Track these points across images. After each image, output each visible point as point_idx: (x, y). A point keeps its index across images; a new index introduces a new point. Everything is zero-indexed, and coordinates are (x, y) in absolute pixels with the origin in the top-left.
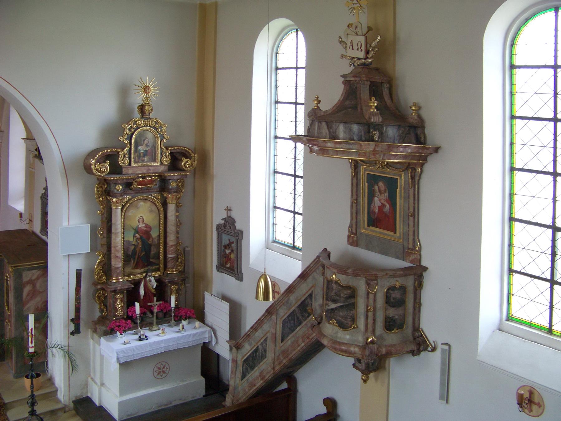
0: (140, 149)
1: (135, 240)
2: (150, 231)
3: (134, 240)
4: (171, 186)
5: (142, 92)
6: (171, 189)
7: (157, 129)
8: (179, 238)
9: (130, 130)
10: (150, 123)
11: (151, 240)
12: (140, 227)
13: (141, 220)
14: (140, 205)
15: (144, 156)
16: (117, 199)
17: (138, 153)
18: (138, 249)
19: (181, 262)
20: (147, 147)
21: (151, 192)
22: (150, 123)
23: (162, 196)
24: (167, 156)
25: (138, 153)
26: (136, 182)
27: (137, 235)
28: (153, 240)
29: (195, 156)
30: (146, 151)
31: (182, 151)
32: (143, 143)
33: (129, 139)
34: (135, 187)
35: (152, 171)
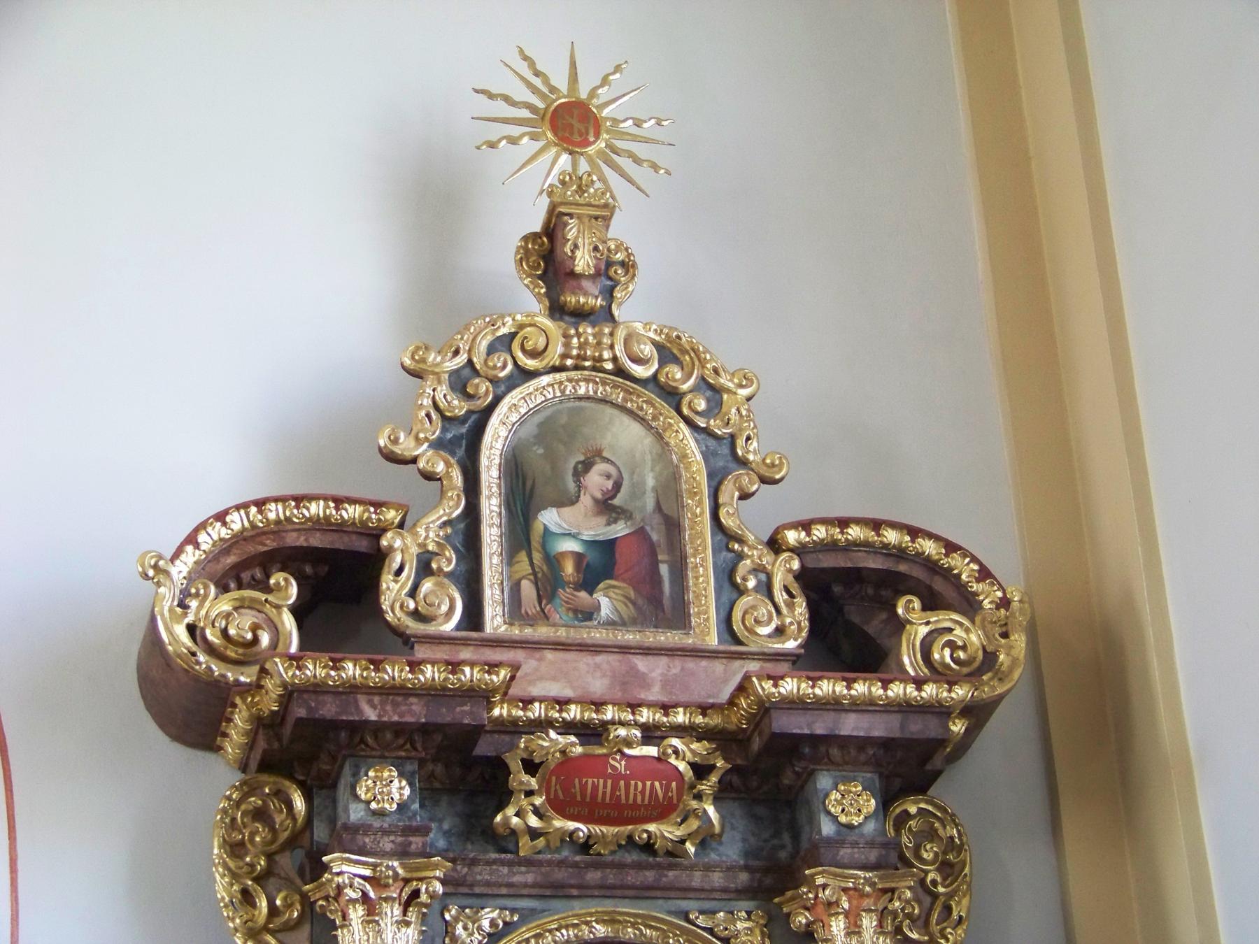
0: (554, 529)
4: (835, 818)
5: (534, 137)
7: (672, 396)
9: (459, 383)
10: (619, 350)
15: (590, 578)
16: (368, 873)
17: (537, 556)
20: (615, 521)
21: (686, 891)
22: (619, 350)
24: (781, 597)
25: (537, 556)
26: (531, 767)
29: (1005, 603)
30: (608, 547)
31: (903, 568)
32: (571, 485)
33: (461, 452)
34: (534, 821)
35: (656, 688)
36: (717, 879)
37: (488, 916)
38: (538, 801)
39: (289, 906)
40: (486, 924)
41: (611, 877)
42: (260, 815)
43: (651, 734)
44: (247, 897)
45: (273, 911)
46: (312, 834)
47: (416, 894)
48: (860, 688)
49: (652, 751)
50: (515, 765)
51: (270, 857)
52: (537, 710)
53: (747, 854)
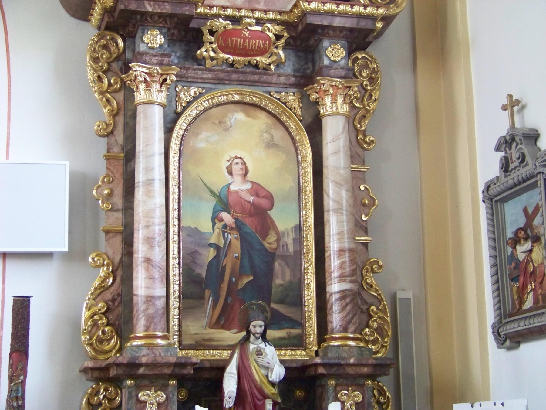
1: (217, 231)
2: (271, 209)
3: (213, 230)
4: (329, 58)
6: (329, 67)
8: (370, 246)
11: (272, 238)
12: (237, 192)
13: (237, 169)
14: (233, 121)
16: (147, 71)
18: (228, 262)
19: (380, 330)
21: (270, 84)
23: (304, 98)
26: (212, 33)
27: (225, 215)
28: (278, 240)
34: (212, 54)
35: (262, 4)
36: (282, 80)
37: (193, 90)
38: (214, 46)
39: (116, 83)
40: (192, 93)
41: (242, 77)
42: (105, 47)
43: (259, 22)
44: (100, 79)
45: (110, 85)
46: (125, 56)
47: (165, 80)
48: (342, 7)
49: (259, 28)
50: (206, 31)
51: (109, 64)
52: (215, 11)
53: (295, 71)
